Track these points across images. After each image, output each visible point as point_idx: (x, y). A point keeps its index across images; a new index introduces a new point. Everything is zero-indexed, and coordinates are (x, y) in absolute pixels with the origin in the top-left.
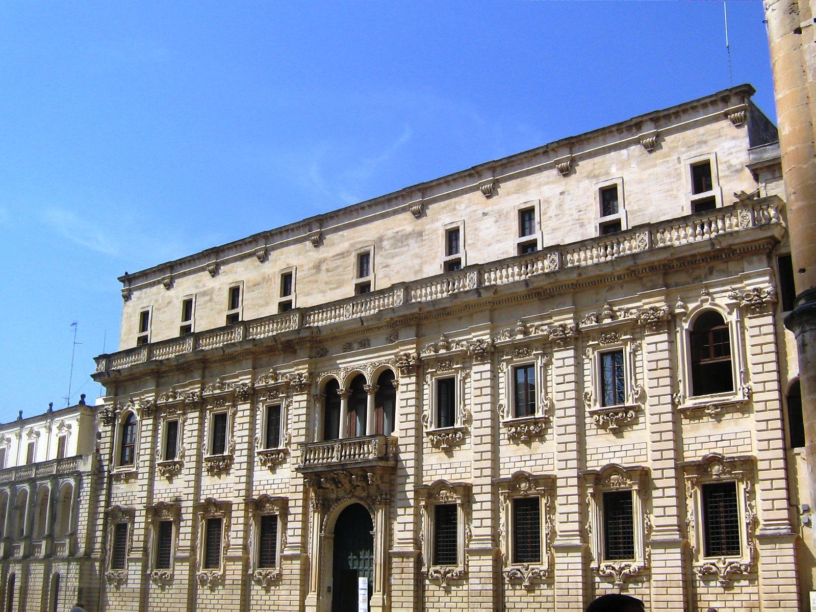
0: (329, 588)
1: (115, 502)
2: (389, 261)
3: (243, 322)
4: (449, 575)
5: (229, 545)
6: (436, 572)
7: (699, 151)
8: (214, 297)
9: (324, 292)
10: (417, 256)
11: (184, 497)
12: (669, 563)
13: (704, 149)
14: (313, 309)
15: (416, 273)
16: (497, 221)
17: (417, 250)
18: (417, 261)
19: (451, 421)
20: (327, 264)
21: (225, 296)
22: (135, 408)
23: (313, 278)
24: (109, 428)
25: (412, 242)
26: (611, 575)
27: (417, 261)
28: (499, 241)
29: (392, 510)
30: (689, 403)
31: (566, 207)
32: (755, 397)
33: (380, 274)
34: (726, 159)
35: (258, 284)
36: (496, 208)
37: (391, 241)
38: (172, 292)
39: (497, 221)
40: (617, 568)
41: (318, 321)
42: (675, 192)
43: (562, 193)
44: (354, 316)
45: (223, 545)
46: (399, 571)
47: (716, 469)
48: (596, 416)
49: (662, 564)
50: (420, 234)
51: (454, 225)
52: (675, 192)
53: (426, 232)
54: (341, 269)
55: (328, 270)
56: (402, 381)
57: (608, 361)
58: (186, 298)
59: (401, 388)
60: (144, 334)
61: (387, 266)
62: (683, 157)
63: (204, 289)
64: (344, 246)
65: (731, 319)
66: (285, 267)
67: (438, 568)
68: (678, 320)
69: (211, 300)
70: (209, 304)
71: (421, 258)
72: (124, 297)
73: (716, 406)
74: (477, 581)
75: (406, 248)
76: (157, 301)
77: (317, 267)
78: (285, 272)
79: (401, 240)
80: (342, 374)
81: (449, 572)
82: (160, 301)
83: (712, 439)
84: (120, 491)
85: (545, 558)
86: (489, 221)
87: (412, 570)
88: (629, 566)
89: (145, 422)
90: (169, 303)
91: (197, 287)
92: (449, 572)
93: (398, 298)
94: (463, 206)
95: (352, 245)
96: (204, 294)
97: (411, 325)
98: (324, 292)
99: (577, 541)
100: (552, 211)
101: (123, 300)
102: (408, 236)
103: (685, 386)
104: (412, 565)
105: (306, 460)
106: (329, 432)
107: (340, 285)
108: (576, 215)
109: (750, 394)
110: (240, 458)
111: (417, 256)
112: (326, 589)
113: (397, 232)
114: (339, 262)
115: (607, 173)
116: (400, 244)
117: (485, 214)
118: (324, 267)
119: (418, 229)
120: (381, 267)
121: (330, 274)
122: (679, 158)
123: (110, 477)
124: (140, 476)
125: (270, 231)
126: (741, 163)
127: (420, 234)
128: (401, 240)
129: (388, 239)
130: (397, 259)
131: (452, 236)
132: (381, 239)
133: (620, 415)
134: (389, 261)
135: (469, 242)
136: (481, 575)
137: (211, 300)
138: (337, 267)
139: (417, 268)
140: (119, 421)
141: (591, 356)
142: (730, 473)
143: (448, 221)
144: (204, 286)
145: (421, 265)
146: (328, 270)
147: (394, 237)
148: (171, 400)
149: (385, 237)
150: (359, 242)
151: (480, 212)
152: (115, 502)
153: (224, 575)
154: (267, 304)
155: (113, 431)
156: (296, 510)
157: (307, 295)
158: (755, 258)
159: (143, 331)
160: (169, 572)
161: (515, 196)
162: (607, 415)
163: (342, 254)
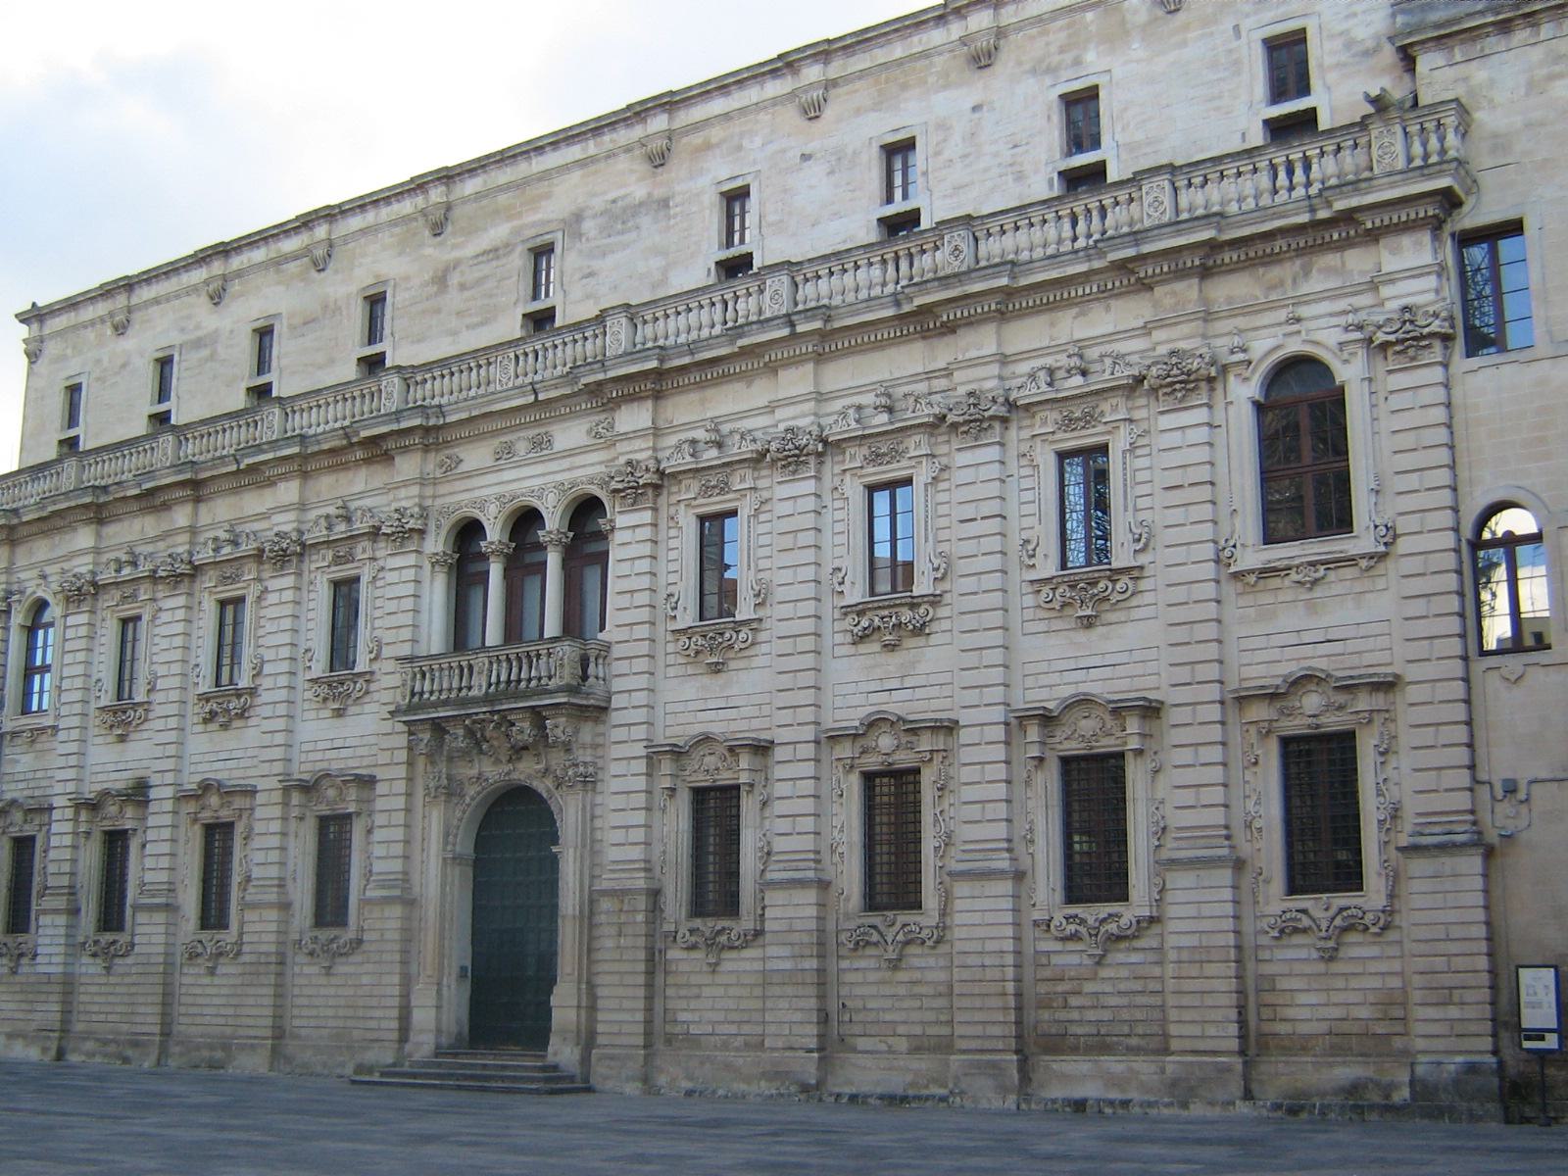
0: (463, 969)
2: (596, 264)
3: (279, 399)
4: (723, 939)
5: (248, 879)
6: (692, 931)
7: (1282, 9)
8: (220, 349)
9: (455, 333)
11: (155, 780)
14: (428, 367)
15: (654, 287)
18: (656, 263)
20: (462, 273)
21: (244, 349)
25: (645, 221)
27: (656, 263)
29: (599, 799)
30: (1255, 555)
32: (1403, 545)
33: (576, 291)
34: (1340, 28)
35: (313, 320)
38: (128, 343)
40: (1091, 921)
41: (437, 390)
44: (519, 381)
45: (236, 879)
46: (613, 931)
47: (1312, 701)
48: (1046, 589)
49: (1191, 910)
50: (664, 203)
53: (678, 199)
55: (463, 287)
56: (621, 521)
57: (1075, 472)
58: (160, 355)
59: (618, 537)
60: (72, 433)
61: (591, 275)
63: (199, 333)
65: (1349, 372)
66: (371, 281)
67: (698, 923)
68: (1231, 378)
72: (28, 354)
73: (1312, 564)
74: (785, 951)
75: (633, 235)
76: (98, 361)
77: (441, 280)
78: (372, 292)
79: (622, 217)
80: (493, 509)
81: (720, 932)
82: (105, 363)
83: (1307, 637)
85: (930, 898)
86: (816, 171)
87: (642, 929)
89: (71, 620)
91: (183, 330)
92: (720, 932)
93: (618, 336)
94: (758, 141)
95: (517, 231)
96: (198, 344)
97: (641, 398)
98: (455, 333)
99: (1003, 863)
101: (25, 360)
103: (1248, 524)
104: (640, 917)
105: (413, 694)
106: (461, 632)
109: (1391, 536)
110: (272, 693)
112: (455, 971)
113: (614, 201)
114: (486, 269)
116: (619, 226)
118: (454, 279)
120: (577, 276)
121: (467, 294)
122: (1236, 28)
124: (62, 735)
125: (339, 206)
126: (1377, 37)
127: (664, 203)
128: (622, 217)
129: (595, 216)
130: (610, 260)
132: (578, 217)
133: (1101, 585)
134: (596, 264)
135: (771, 218)
136: (795, 937)
137: (212, 357)
138: (480, 281)
141: (1039, 460)
142: (1341, 708)
144: (198, 327)
145: (665, 271)
148: (127, 571)
149: (589, 213)
150: (534, 225)
153: (240, 943)
154: (332, 361)
156: (389, 799)
157: (419, 341)
159: (69, 427)
160: (123, 938)
162: (1072, 587)
163: (496, 250)
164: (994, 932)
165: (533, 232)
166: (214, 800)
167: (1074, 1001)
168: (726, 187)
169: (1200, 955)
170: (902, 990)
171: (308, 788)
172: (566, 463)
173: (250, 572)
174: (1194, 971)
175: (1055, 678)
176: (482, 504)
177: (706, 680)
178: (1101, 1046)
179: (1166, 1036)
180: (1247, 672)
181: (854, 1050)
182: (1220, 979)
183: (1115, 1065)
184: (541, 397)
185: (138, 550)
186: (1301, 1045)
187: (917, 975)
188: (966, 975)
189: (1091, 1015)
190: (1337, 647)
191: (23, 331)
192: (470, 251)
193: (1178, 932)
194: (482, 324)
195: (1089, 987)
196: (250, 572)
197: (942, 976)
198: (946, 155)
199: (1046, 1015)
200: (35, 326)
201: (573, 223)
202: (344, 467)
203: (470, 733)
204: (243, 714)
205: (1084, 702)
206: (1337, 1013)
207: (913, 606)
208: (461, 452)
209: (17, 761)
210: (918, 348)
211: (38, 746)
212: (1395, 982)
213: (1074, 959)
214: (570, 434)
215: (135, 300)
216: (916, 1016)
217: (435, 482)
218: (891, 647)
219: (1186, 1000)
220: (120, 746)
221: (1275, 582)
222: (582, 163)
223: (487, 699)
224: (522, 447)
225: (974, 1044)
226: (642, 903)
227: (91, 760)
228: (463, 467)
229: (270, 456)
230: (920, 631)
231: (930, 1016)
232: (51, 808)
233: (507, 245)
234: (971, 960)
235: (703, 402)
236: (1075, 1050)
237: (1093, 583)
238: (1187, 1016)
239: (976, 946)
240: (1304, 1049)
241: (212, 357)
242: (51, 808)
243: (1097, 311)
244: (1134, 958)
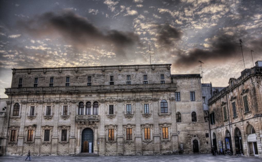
1: (11, 125)
2: (96, 80)
8: (45, 79)
9: (79, 83)
10: (103, 80)
12: (157, 140)
13: (163, 72)
16: (122, 76)
17: (103, 78)
19: (113, 113)
22: (19, 101)
23: (75, 79)
24: (9, 106)
26: (146, 142)
27: (103, 81)
28: (122, 80)
30: (160, 114)
31: (137, 77)
36: (122, 74)
37: (97, 75)
39: (122, 76)
42: (157, 78)
43: (136, 74)
50: (104, 75)
51: (112, 75)
52: (157, 78)
54: (83, 79)
55: (80, 79)
61: (96, 80)
62: (159, 73)
64: (85, 74)
69: (44, 79)
70: (44, 80)
71: (104, 80)
77: (77, 77)
84: (13, 122)
88: (150, 140)
89: (23, 106)
90: (30, 78)
94: (114, 72)
95: (87, 74)
96: (42, 77)
100: (134, 77)
102: (101, 75)
104: (104, 140)
107: (83, 82)
108: (139, 79)
111: (103, 80)
114: (83, 77)
115: (145, 72)
117: (119, 74)
118: (79, 78)
119: (103, 74)
123: (9, 118)
127: (104, 75)
128: (99, 76)
129: (96, 75)
130: (98, 79)
131: (112, 77)
134: (96, 80)
135: (116, 79)
136: (120, 142)
139: (103, 82)
140: (13, 105)
143: (111, 74)
145: (104, 82)
146: (80, 79)
147: (97, 75)
151: (118, 74)
152: (11, 125)
155: (11, 107)
158: (172, 92)
161: (126, 72)
163: (84, 76)
164: (139, 142)
165: (89, 75)
166: (47, 127)
167: (146, 147)
168: (111, 75)
169: (157, 143)
170: (130, 146)
171: (61, 127)
172: (94, 98)
173: (52, 104)
174: (156, 144)
175: (144, 122)
176: (84, 100)
177: (110, 119)
178: (148, 150)
179: (154, 149)
180: (160, 122)
181: (126, 151)
182: (158, 145)
183: (150, 152)
184: (92, 92)
185: (34, 99)
186: (164, 150)
187: (132, 145)
188: (137, 145)
189: (147, 148)
190: (166, 121)
191: (12, 71)
192: (81, 75)
193: (155, 142)
194: (82, 83)
195: (147, 146)
196: (52, 104)
197: (134, 145)
198: (133, 77)
199: (143, 148)
200: (14, 70)
201: (94, 75)
202: (66, 94)
203: (84, 123)
204: (51, 119)
205: (147, 124)
206: (167, 147)
207: (131, 115)
208: (81, 95)
209: (13, 121)
210: (132, 94)
211: (17, 120)
212: (171, 145)
213: (146, 144)
214: (94, 96)
215: (31, 71)
216: (132, 148)
217: (78, 98)
218: (129, 118)
219: (156, 147)
220: (31, 121)
221: (162, 116)
222: (95, 70)
223: (88, 120)
224: (89, 96)
225: (138, 151)
226: (104, 139)
227: (26, 122)
228: (81, 97)
229: (57, 92)
230: (132, 117)
231: (133, 148)
232: (20, 127)
233: (85, 75)
234: (138, 144)
235: (110, 95)
236: (146, 151)
237: (148, 115)
238: (156, 148)
239: (138, 143)
240: (164, 150)
241: (44, 79)
242: (20, 127)
243: (148, 93)
244: (151, 144)
